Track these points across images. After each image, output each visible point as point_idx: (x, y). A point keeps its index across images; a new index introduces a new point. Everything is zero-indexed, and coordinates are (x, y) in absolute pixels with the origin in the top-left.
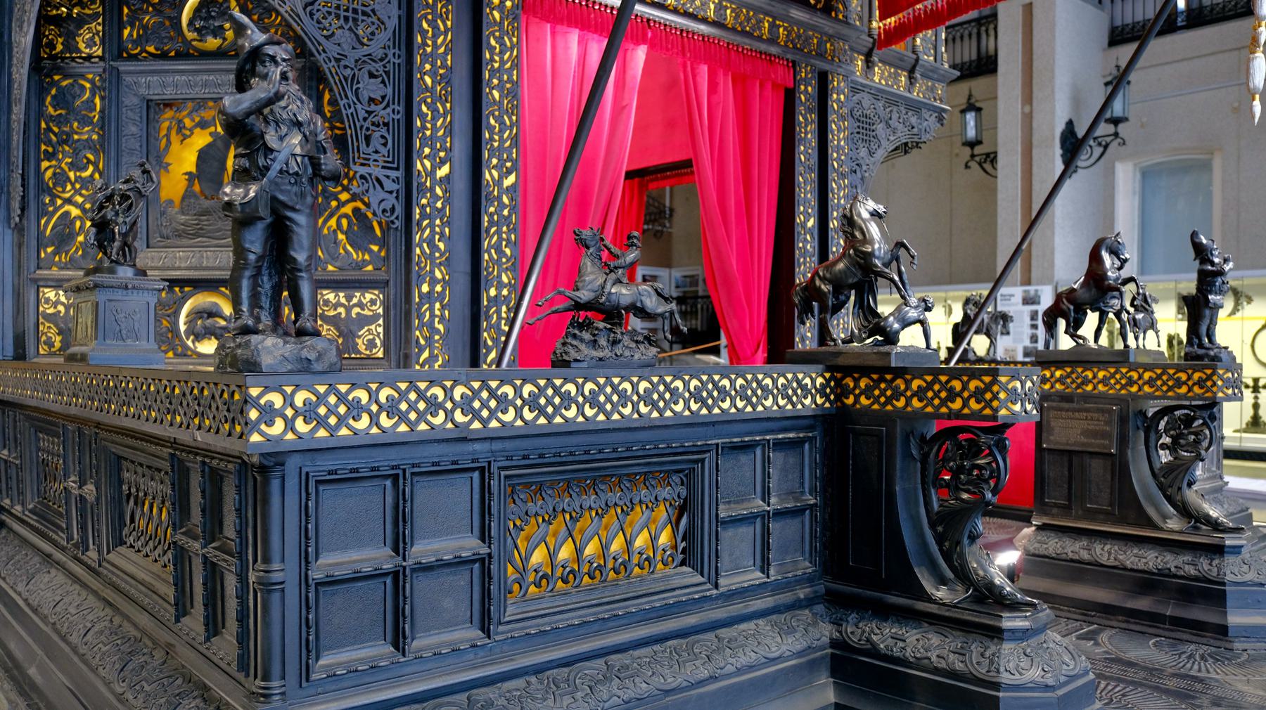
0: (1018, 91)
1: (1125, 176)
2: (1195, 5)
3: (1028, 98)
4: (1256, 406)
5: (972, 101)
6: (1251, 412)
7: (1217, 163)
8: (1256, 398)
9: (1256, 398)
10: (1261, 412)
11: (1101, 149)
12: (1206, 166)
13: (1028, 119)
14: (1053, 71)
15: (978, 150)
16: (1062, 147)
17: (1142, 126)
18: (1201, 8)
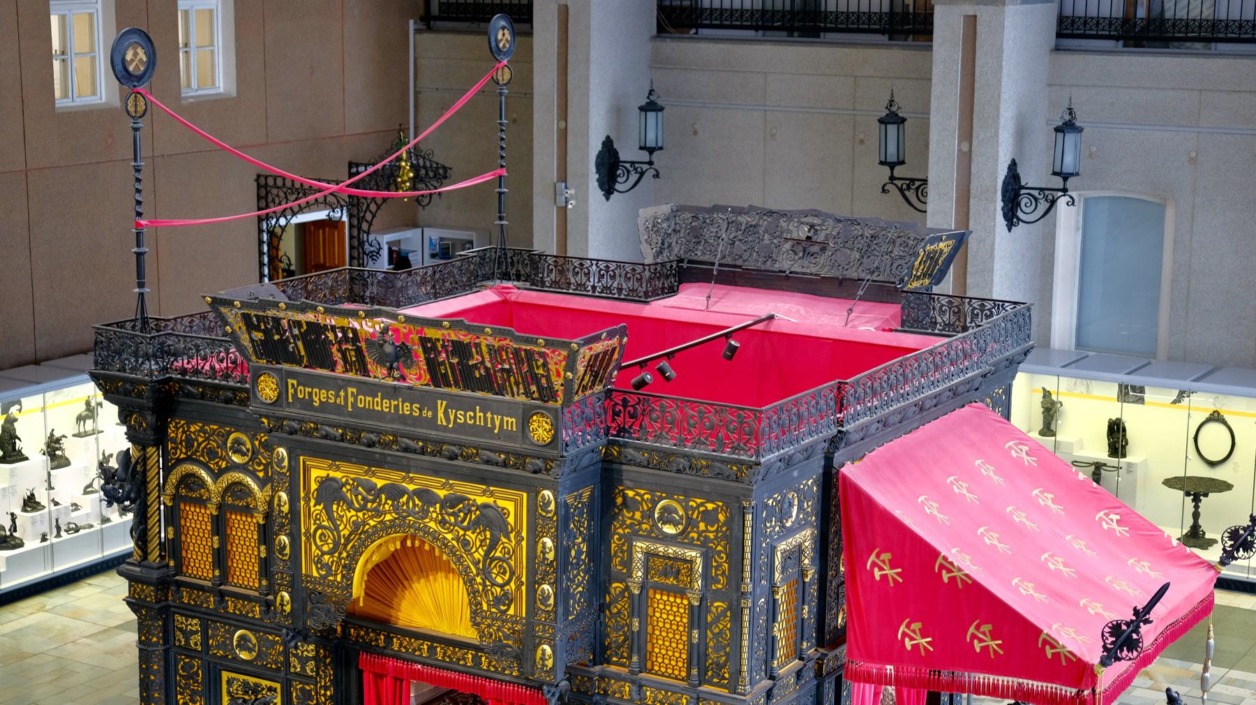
0: (955, 123)
1: (1066, 215)
2: (1156, 11)
3: (967, 133)
4: (1196, 515)
5: (894, 109)
6: (1189, 522)
7: (1170, 213)
8: (1197, 507)
9: (1197, 507)
10: (1201, 522)
11: (1043, 206)
12: (1159, 211)
13: (966, 160)
14: (997, 109)
15: (899, 171)
16: (1004, 196)
17: (1091, 156)
18: (1162, 20)
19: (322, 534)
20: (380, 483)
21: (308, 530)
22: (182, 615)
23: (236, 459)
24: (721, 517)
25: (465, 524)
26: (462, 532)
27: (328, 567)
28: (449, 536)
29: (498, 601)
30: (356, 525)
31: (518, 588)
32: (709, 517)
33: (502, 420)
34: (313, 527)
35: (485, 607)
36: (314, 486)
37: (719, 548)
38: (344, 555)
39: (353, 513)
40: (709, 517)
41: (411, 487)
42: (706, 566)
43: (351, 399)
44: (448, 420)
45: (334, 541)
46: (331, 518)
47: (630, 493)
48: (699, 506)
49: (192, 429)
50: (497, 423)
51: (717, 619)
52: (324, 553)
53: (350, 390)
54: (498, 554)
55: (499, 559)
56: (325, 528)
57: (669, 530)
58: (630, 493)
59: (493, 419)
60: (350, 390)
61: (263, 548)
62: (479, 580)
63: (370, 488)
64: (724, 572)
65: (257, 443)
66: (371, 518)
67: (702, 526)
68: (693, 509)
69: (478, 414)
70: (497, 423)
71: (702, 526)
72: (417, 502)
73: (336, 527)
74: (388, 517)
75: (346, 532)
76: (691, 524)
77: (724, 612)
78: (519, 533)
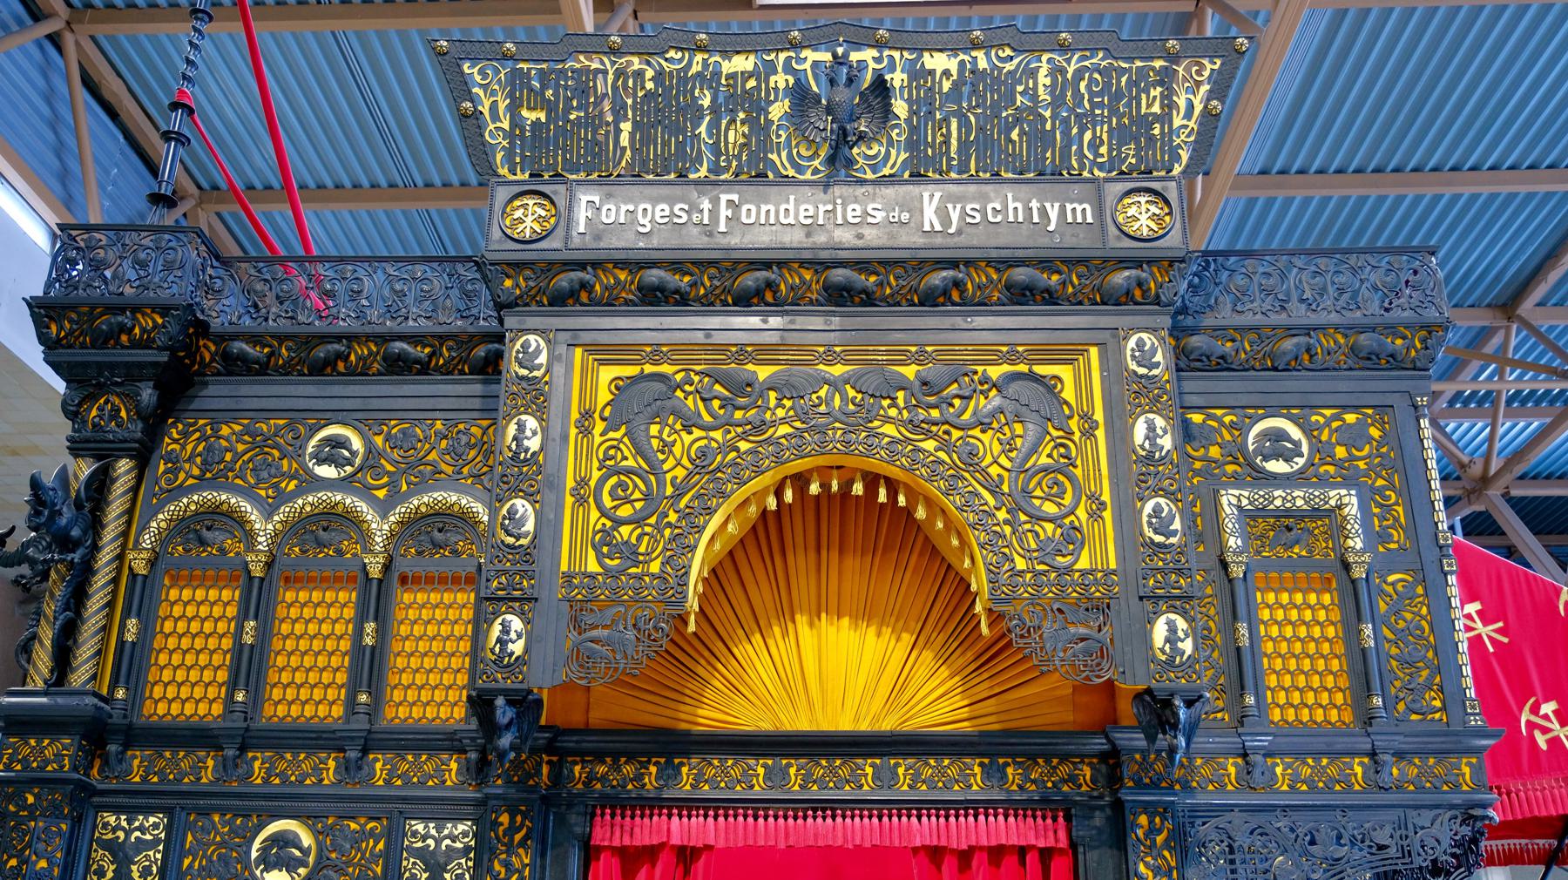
19: (620, 484)
20: (763, 373)
21: (582, 482)
22: (117, 810)
23: (327, 472)
24: (1375, 432)
25: (966, 416)
26: (956, 434)
27: (630, 553)
28: (930, 445)
29: (1047, 550)
30: (703, 453)
31: (1095, 516)
32: (1354, 438)
33: (1063, 210)
34: (596, 475)
35: (1021, 564)
36: (604, 396)
37: (1380, 482)
38: (673, 517)
39: (697, 433)
40: (1354, 438)
41: (838, 370)
42: (1363, 507)
43: (724, 212)
44: (946, 221)
45: (647, 497)
46: (640, 451)
47: (1197, 418)
49: (225, 431)
50: (1054, 215)
52: (620, 522)
53: (724, 198)
54: (1044, 460)
55: (1045, 470)
56: (629, 472)
57: (1276, 466)
58: (1197, 418)
59: (1043, 212)
60: (724, 198)
61: (370, 627)
62: (1002, 515)
63: (742, 388)
64: (1396, 520)
65: (379, 440)
66: (743, 437)
67: (1341, 452)
69: (1011, 206)
70: (1054, 215)
71: (1341, 452)
72: (851, 393)
73: (655, 469)
74: (784, 430)
75: (680, 473)
76: (1321, 451)
77: (1410, 587)
78: (1086, 417)
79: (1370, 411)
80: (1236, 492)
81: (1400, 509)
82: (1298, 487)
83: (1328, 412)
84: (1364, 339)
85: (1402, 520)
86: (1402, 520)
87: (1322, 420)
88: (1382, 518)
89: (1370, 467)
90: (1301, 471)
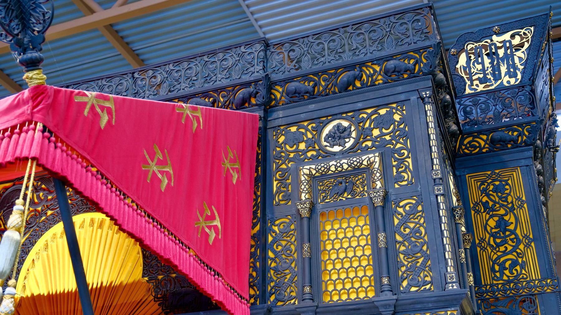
24: (397, 117)
37: (399, 146)
40: (382, 123)
48: (369, 116)
51: (404, 222)
64: (407, 167)
67: (376, 132)
68: (364, 121)
79: (394, 105)
80: (308, 167)
81: (410, 160)
82: (344, 158)
83: (369, 111)
84: (391, 64)
85: (411, 167)
86: (411, 167)
87: (365, 116)
88: (398, 167)
89: (393, 138)
90: (351, 148)
